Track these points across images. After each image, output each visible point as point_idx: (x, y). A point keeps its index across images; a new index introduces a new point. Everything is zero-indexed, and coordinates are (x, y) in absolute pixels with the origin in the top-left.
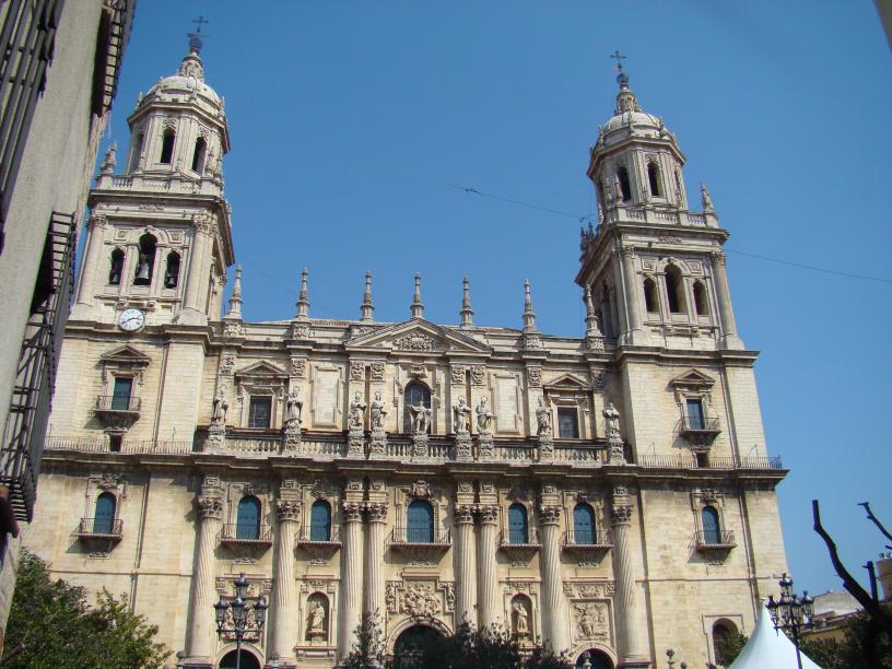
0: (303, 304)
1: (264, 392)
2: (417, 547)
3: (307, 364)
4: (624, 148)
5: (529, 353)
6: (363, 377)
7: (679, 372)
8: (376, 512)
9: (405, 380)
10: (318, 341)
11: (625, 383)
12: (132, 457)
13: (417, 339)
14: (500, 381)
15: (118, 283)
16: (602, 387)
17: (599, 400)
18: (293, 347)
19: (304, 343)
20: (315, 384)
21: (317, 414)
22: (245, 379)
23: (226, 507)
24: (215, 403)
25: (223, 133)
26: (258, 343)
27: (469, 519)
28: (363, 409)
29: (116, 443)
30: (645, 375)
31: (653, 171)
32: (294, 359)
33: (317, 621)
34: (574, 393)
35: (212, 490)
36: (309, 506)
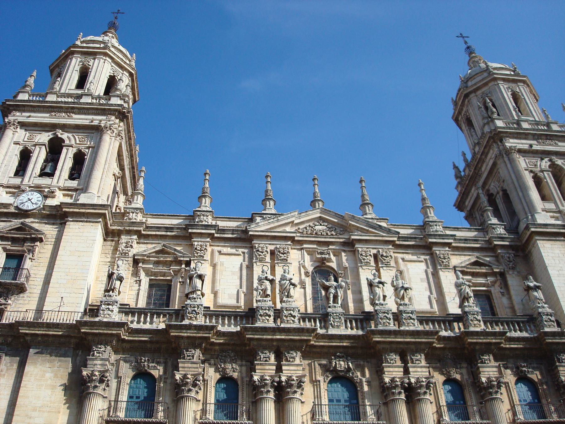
0: (205, 197)
3: (209, 249)
5: (435, 236)
8: (291, 386)
11: (536, 262)
12: (11, 326)
13: (320, 227)
14: (409, 264)
15: (23, 175)
16: (513, 268)
19: (207, 227)
20: (218, 267)
21: (220, 295)
22: (144, 262)
23: (114, 384)
24: (110, 276)
27: (400, 393)
30: (557, 251)
31: (516, 97)
32: (196, 243)
34: (485, 275)
35: (99, 362)
36: (212, 384)
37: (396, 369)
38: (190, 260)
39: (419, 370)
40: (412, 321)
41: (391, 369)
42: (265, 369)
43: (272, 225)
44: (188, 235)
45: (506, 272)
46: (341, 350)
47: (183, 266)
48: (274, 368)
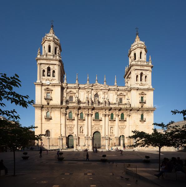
4: (136, 49)
7: (140, 92)
19: (77, 87)
25: (60, 46)
26: (70, 87)
29: (48, 104)
33: (81, 130)
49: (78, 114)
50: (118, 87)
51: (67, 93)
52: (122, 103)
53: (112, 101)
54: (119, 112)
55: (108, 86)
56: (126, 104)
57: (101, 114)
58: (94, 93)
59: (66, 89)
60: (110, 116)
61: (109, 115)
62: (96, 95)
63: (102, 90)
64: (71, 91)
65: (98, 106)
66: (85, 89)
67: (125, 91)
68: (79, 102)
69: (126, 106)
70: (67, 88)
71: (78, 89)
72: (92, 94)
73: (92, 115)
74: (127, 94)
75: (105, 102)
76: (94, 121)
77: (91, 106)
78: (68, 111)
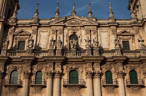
1: (23, 39)
2: (72, 86)
6: (56, 33)
9: (70, 33)
10: (40, 23)
17: (137, 37)
18: (32, 25)
26: (21, 24)
28: (54, 41)
37: (90, 68)
38: (31, 34)
39: (97, 68)
40: (97, 53)
41: (89, 68)
42: (50, 69)
43: (57, 22)
44: (30, 26)
45: (135, 35)
46: (74, 62)
47: (29, 36)
48: (53, 68)
49: (31, 74)
50: (117, 22)
51: (14, 36)
52: (129, 49)
53: (107, 47)
54: (125, 68)
55: (97, 20)
56: (137, 51)
57: (82, 72)
58: (68, 32)
59: (13, 27)
60: (103, 77)
61: (101, 75)
62: (74, 36)
63: (84, 26)
64: (22, 32)
65: (75, 57)
66: (50, 26)
67: (132, 27)
68: (37, 50)
69: (138, 55)
70: (16, 27)
71: (36, 27)
72: (65, 34)
73: (62, 75)
74: (137, 32)
75: (92, 49)
76: (67, 89)
77: (61, 55)
78: (10, 68)
